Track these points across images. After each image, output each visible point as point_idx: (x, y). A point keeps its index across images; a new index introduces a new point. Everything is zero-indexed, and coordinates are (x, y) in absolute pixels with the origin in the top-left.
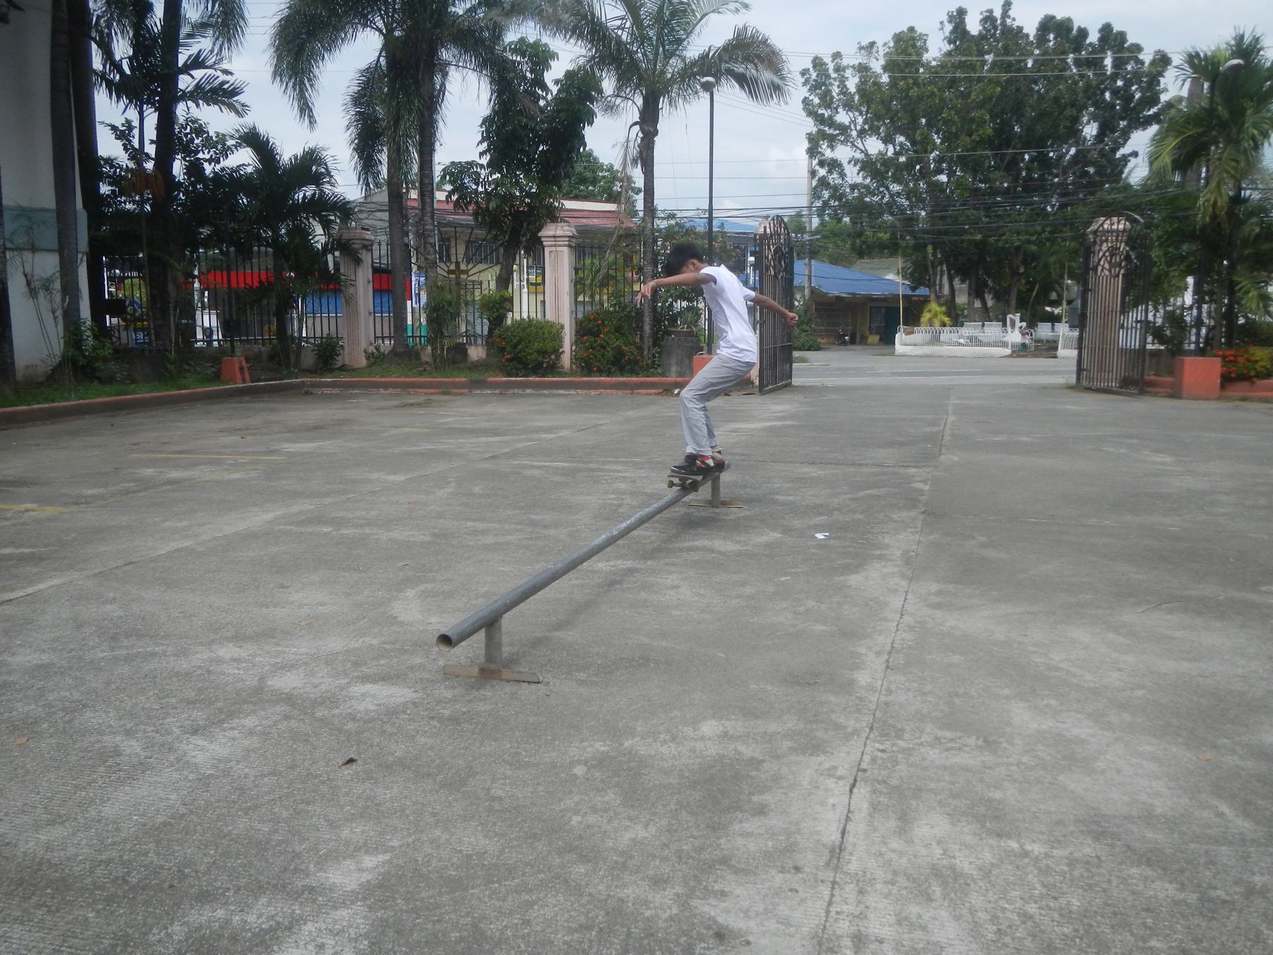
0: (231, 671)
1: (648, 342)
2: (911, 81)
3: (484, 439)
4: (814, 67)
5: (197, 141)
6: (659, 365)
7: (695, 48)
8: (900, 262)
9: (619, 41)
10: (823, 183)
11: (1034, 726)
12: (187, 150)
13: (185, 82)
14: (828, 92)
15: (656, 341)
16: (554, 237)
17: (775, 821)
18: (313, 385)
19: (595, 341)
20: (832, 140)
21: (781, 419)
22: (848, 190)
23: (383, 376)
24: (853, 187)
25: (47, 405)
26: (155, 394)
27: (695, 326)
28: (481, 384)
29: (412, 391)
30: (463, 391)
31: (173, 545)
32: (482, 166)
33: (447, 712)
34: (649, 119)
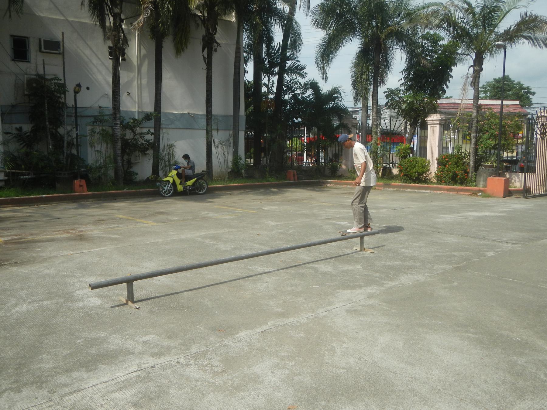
0: (77, 285)
1: (471, 169)
3: (343, 210)
5: (294, 87)
6: (475, 181)
7: (503, 27)
11: (258, 371)
12: (290, 89)
13: (287, 66)
16: (433, 120)
17: (85, 375)
18: (323, 183)
19: (444, 169)
21: (505, 212)
25: (214, 186)
28: (388, 186)
30: (381, 188)
31: (157, 240)
33: (93, 312)
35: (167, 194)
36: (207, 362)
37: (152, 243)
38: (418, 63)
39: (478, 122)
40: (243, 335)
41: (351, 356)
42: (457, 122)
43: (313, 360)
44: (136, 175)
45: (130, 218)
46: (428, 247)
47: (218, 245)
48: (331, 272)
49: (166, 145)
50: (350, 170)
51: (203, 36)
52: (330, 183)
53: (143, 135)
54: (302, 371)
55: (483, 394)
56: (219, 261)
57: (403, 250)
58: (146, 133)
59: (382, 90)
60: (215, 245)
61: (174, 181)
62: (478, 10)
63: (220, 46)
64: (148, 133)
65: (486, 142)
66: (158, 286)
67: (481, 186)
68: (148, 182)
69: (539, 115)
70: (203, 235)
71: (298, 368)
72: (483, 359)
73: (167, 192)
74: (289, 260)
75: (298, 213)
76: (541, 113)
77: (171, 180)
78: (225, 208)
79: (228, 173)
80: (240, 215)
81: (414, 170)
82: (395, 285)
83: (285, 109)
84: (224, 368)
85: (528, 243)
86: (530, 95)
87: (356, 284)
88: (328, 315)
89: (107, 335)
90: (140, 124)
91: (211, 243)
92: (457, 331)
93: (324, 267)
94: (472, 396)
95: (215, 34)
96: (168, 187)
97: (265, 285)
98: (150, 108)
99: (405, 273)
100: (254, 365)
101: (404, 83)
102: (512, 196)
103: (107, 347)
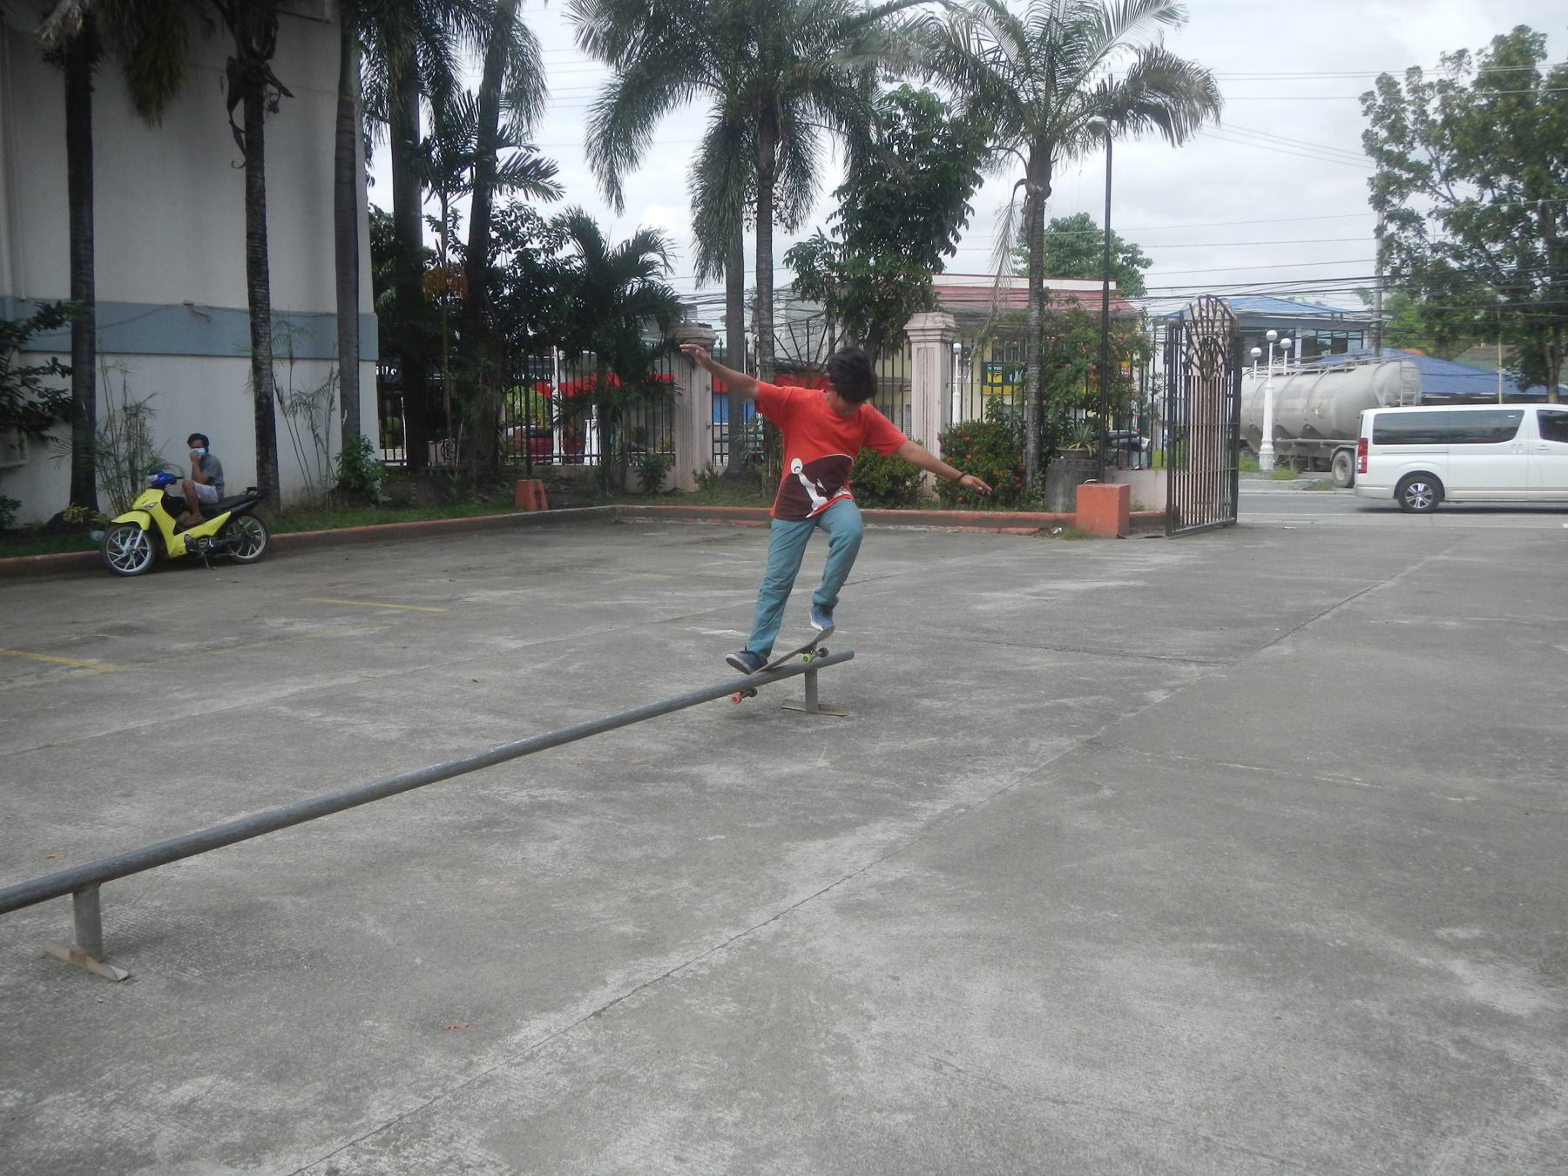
2: (1513, 100)
3: (707, 594)
4: (1380, 88)
5: (523, 230)
6: (1043, 496)
8: (1500, 350)
9: (994, 75)
10: (1388, 245)
11: (630, 1159)
12: (511, 237)
14: (1400, 119)
15: (1044, 460)
16: (923, 330)
20: (1403, 187)
22: (1428, 253)
23: (709, 504)
24: (1435, 248)
25: (290, 535)
26: (422, 523)
27: (1092, 445)
29: (733, 522)
31: (132, 724)
32: (837, 246)
34: (1039, 172)
35: (131, 567)
36: (441, 1155)
37: (118, 733)
38: (880, 170)
39: (1042, 332)
40: (534, 1033)
41: (908, 1060)
42: (990, 333)
43: (798, 1093)
44: (14, 509)
45: (13, 653)
46: (988, 688)
47: (352, 725)
48: (743, 786)
49: (118, 406)
50: (699, 472)
51: (230, 59)
52: (646, 513)
53: (34, 376)
54: (775, 1137)
55: (1330, 1132)
56: (394, 782)
57: (926, 702)
58: (43, 368)
59: (782, 242)
60: (342, 725)
61: (153, 522)
62: (1034, 30)
63: (289, 95)
64: (52, 370)
65: (1066, 390)
66: (178, 888)
67: (1059, 508)
68: (58, 530)
69: (1196, 314)
70: (293, 695)
71: (758, 1130)
72: (1279, 1018)
73: (132, 559)
74: (605, 759)
75: (577, 606)
76: (1201, 309)
77: (143, 521)
78: (339, 602)
79: (333, 491)
80: (396, 622)
81: (883, 469)
82: (945, 811)
83: (496, 296)
84: (506, 1166)
85: (1235, 660)
86: (1139, 268)
87: (832, 817)
88: (787, 929)
89: (24, 1100)
90: (22, 338)
91: (328, 719)
92: (1174, 938)
93: (723, 774)
94: (1304, 1144)
95: (270, 55)
96: (133, 542)
97: (553, 847)
98: (55, 286)
99: (958, 770)
100: (608, 1142)
101: (842, 225)
102: (1137, 532)
103: (37, 1150)
